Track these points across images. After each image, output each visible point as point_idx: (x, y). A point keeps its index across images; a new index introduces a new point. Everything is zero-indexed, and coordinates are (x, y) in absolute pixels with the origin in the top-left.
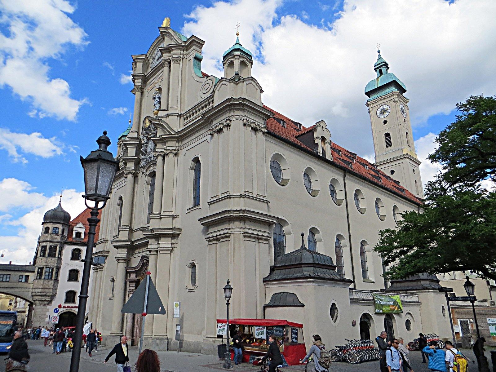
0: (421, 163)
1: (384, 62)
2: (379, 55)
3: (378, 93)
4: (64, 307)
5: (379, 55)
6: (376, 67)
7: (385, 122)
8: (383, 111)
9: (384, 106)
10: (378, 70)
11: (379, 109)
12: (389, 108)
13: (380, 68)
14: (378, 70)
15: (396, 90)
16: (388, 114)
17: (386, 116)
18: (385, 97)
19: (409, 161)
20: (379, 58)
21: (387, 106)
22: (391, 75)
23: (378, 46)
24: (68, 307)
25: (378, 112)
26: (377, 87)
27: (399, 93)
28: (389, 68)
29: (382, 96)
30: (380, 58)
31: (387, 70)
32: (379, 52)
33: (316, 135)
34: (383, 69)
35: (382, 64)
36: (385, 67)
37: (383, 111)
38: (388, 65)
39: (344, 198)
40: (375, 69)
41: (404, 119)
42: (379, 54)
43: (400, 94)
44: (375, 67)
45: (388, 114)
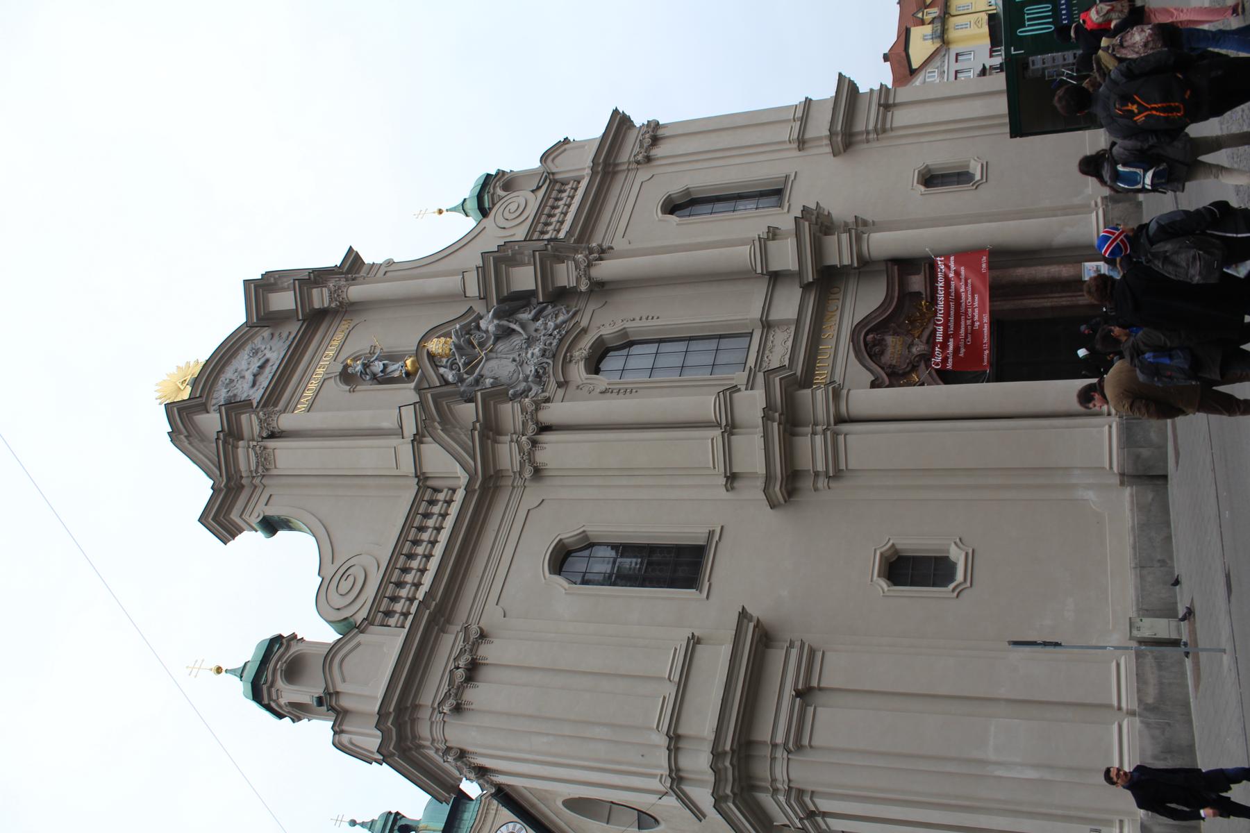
2: (363, 825)
5: (363, 825)
13: (396, 828)
18: (479, 821)
23: (338, 821)
29: (471, 827)
32: (353, 823)
42: (359, 824)
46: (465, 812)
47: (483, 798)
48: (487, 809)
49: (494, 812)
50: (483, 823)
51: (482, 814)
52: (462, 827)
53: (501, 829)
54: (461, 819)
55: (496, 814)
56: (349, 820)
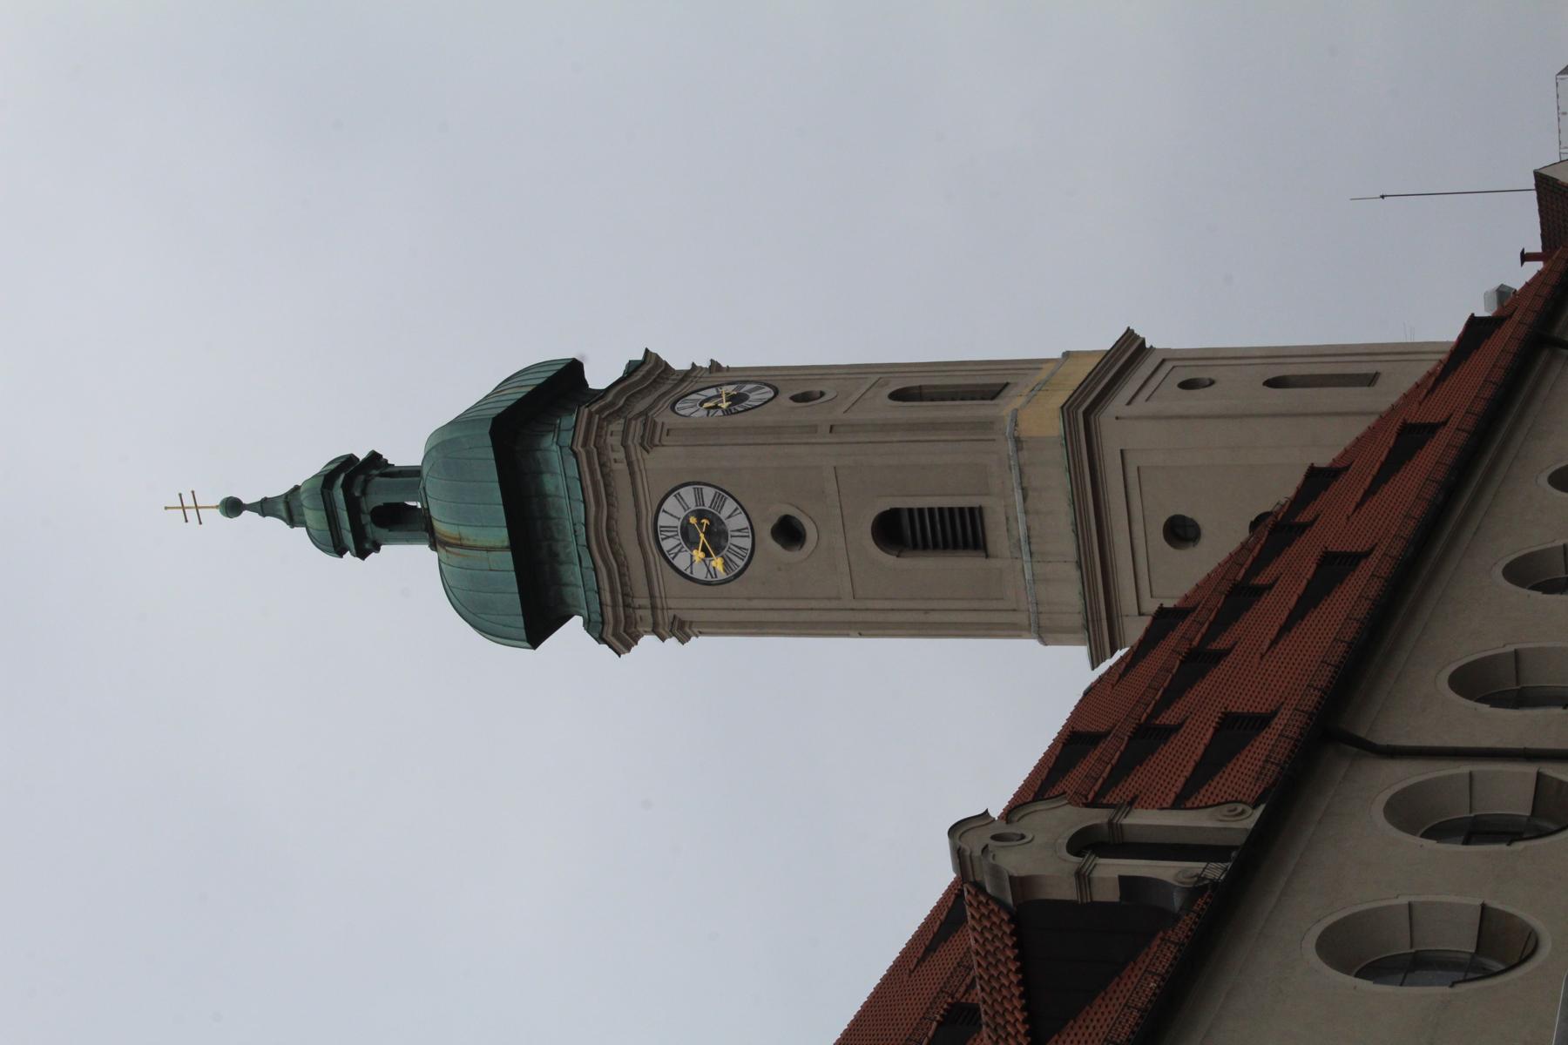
0: (1129, 335)
1: (328, 478)
2: (265, 507)
3: (554, 555)
5: (265, 507)
6: (348, 538)
7: (789, 532)
9: (663, 520)
10: (372, 530)
11: (682, 562)
12: (688, 493)
13: (366, 519)
14: (372, 530)
15: (567, 421)
16: (730, 505)
17: (740, 521)
19: (1117, 404)
20: (284, 514)
21: (671, 501)
22: (446, 442)
23: (188, 507)
25: (700, 573)
26: (509, 554)
27: (595, 407)
28: (375, 458)
30: (282, 507)
31: (389, 470)
32: (233, 507)
33: (1066, 891)
34: (378, 497)
35: (339, 495)
36: (366, 482)
38: (351, 459)
39: (1531, 769)
40: (362, 554)
41: (795, 399)
42: (252, 507)
43: (602, 403)
44: (340, 552)
45: (730, 505)
46: (541, 473)
47: (579, 448)
48: (602, 465)
49: (623, 466)
50: (609, 505)
51: (595, 483)
52: (553, 514)
53: (666, 506)
54: (542, 495)
55: (632, 474)
56: (218, 504)
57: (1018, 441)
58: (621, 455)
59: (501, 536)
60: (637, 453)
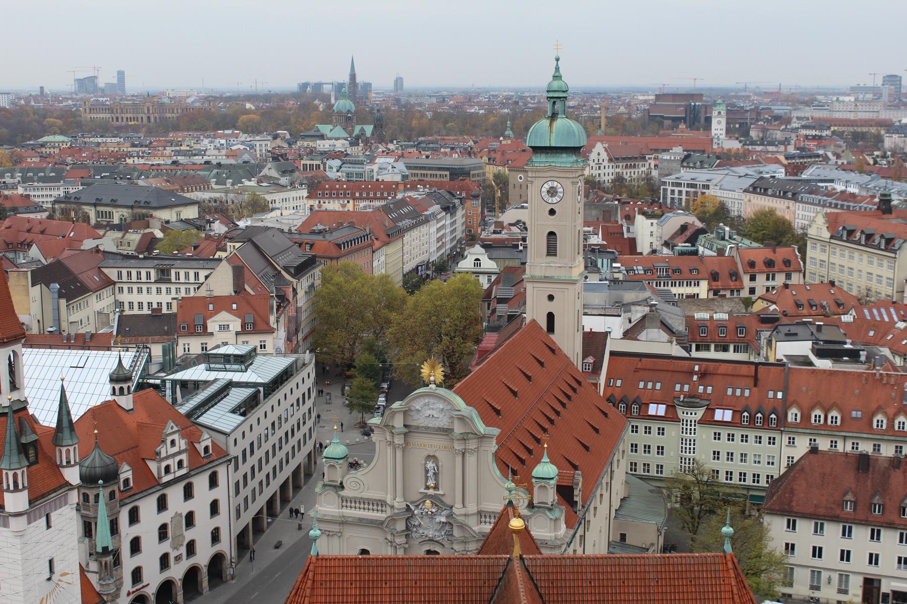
2: (557, 69)
3: (547, 153)
4: (133, 592)
5: (557, 69)
6: (551, 95)
7: (552, 212)
8: (552, 192)
9: (555, 183)
11: (546, 185)
13: (555, 100)
14: (552, 100)
17: (555, 201)
24: (137, 590)
25: (543, 189)
32: (557, 60)
37: (552, 192)
42: (557, 65)
57: (571, 267)
58: (571, 176)
59: (553, 145)
60: (571, 180)
